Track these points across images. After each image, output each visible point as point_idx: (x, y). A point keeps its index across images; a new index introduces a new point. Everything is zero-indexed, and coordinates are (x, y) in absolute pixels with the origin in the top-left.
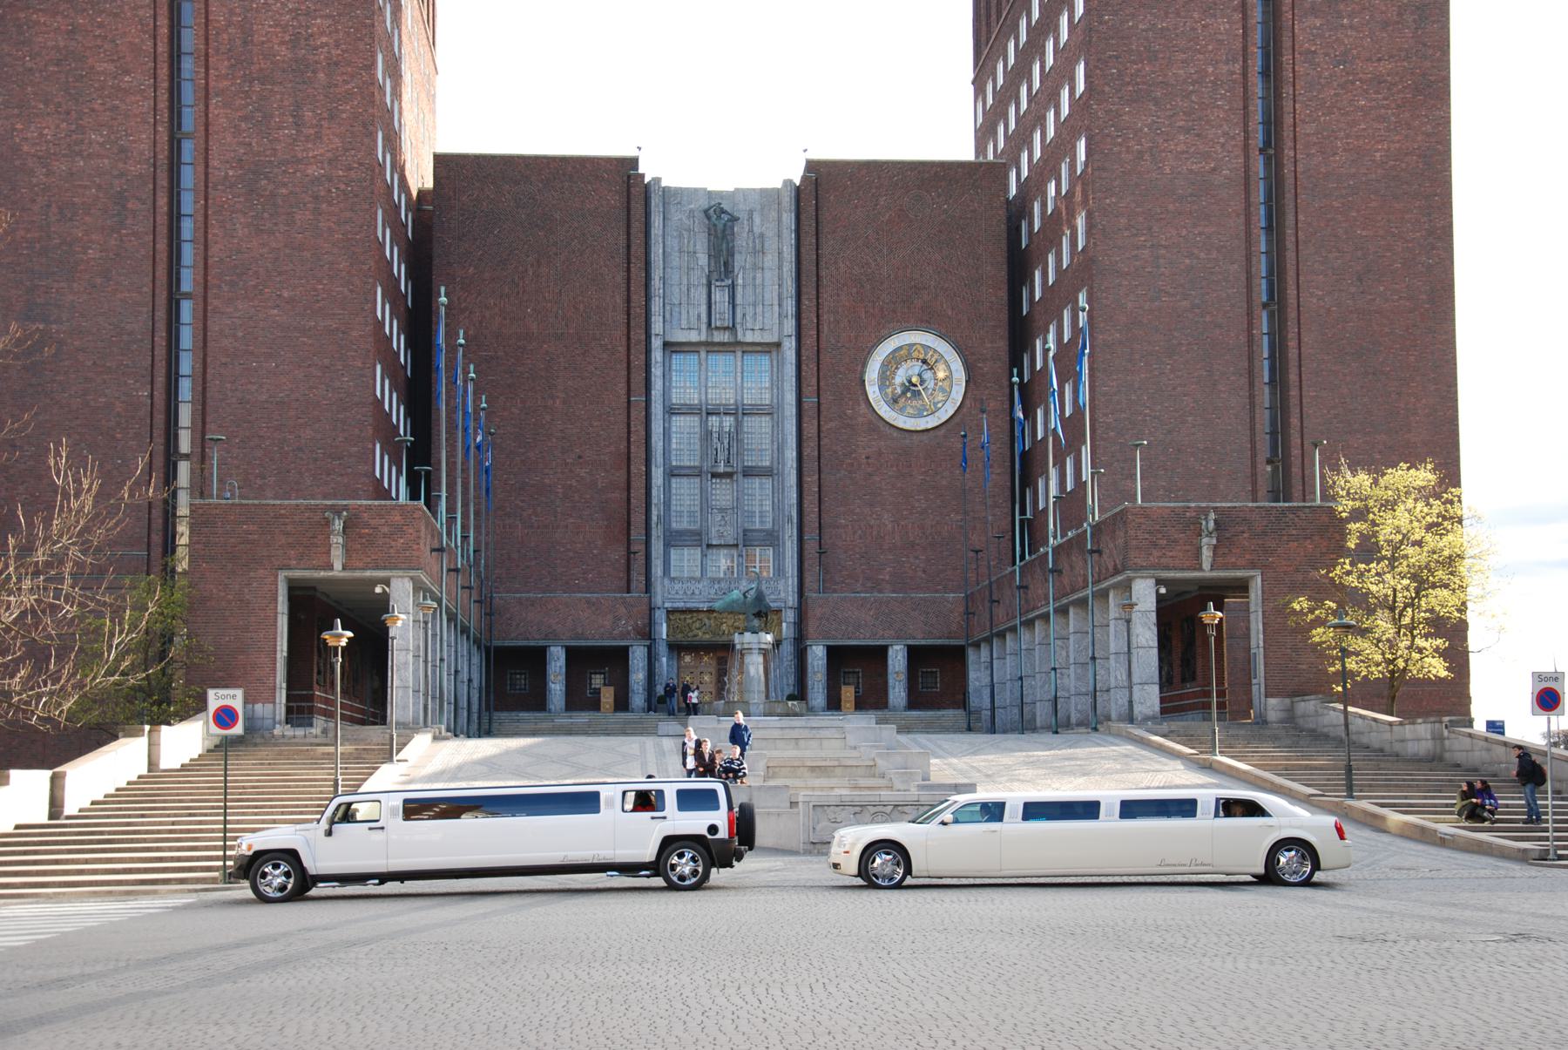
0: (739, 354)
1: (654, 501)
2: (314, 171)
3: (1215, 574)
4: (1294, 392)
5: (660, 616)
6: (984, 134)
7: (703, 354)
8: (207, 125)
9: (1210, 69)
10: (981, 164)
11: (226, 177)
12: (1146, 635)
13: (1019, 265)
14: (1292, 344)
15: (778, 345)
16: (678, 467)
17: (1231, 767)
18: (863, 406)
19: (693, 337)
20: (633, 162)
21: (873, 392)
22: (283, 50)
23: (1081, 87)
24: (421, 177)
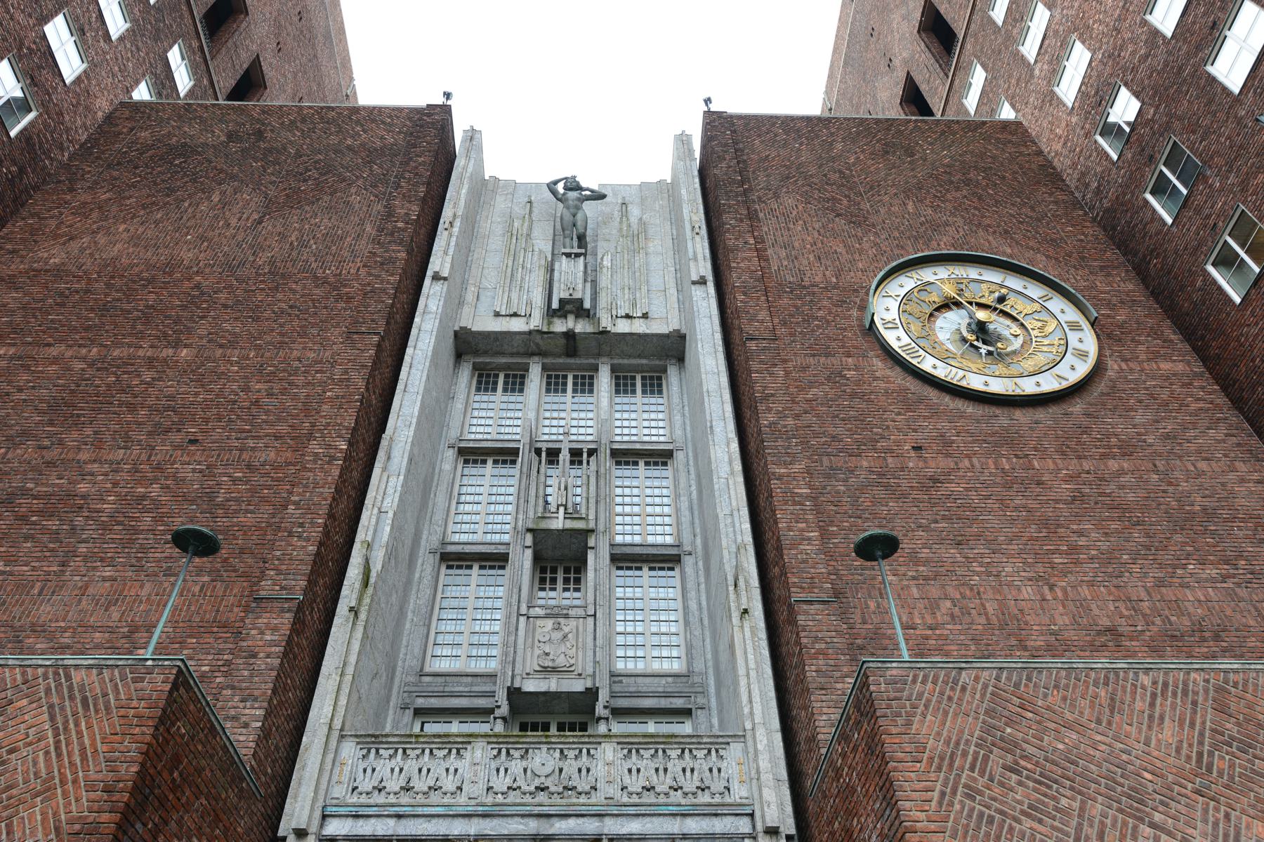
15: (673, 349)
19: (517, 325)
21: (896, 339)
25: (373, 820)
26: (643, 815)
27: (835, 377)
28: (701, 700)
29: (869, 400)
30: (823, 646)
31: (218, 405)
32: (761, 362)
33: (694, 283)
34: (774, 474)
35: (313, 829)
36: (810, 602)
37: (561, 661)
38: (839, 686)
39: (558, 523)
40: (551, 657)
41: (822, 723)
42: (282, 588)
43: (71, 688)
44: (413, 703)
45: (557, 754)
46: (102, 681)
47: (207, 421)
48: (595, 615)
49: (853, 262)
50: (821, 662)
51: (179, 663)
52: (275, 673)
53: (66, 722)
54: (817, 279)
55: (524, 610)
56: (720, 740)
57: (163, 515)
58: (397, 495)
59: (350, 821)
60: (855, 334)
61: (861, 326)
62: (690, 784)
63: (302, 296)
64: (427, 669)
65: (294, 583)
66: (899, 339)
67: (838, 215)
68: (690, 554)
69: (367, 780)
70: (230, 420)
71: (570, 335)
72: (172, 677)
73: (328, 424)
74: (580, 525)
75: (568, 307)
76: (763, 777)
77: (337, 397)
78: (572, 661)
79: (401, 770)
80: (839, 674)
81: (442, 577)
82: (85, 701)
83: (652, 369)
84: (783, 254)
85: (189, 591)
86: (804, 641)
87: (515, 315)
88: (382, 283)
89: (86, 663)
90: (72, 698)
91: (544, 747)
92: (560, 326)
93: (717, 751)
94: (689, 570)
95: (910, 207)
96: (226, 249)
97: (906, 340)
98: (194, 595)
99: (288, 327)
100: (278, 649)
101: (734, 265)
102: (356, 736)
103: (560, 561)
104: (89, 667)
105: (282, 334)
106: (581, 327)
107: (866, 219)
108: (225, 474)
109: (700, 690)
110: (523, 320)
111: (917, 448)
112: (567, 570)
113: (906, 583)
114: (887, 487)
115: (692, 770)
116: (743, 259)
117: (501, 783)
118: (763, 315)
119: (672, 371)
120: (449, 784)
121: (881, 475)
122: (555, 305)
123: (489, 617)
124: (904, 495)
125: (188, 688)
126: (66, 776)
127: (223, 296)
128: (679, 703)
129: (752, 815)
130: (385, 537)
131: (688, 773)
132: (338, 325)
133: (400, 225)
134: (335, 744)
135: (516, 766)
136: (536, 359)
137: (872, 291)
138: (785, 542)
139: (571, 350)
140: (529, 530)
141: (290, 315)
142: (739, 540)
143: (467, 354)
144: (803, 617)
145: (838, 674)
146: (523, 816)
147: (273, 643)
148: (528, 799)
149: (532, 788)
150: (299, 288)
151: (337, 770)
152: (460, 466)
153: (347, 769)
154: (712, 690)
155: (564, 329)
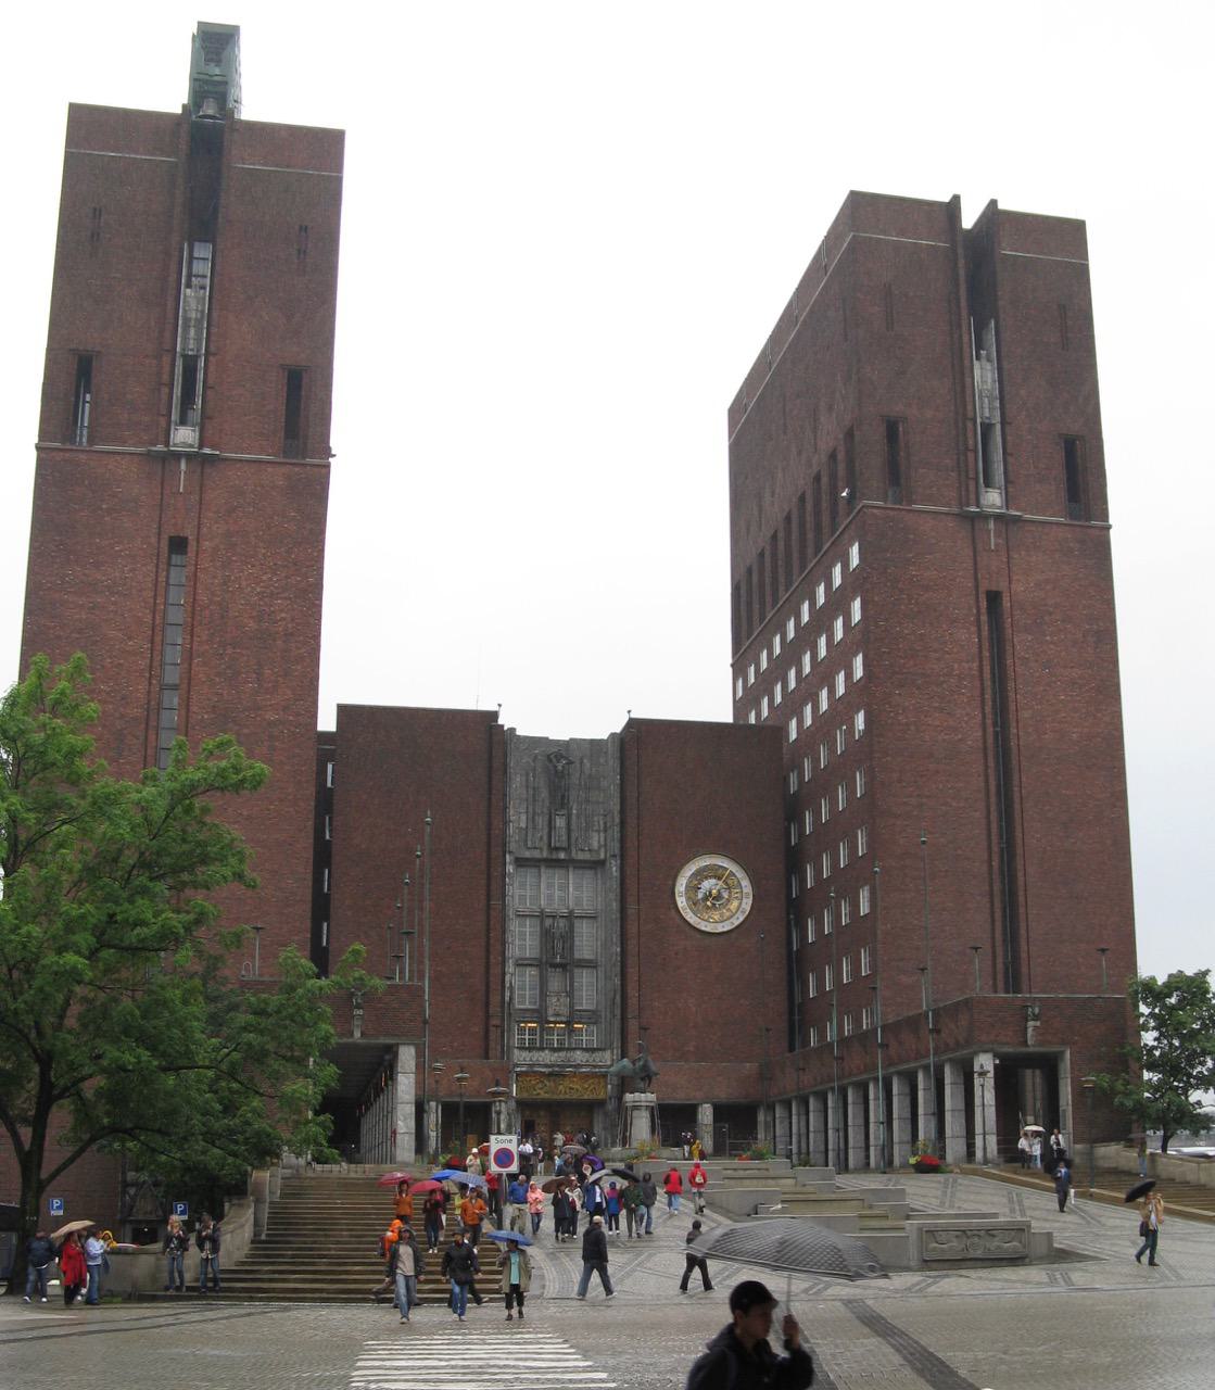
0: (571, 869)
2: (271, 716)
3: (1037, 1049)
4: (1022, 910)
6: (740, 707)
7: (542, 870)
8: (190, 679)
9: (956, 666)
10: (741, 727)
11: (202, 720)
12: (986, 1094)
13: (793, 809)
14: (1020, 874)
15: (602, 863)
16: (580, 960)
17: (1110, 1196)
18: (673, 912)
19: (537, 854)
20: (494, 715)
21: (681, 902)
22: (252, 624)
23: (859, 672)
24: (327, 722)
97: (685, 903)
120: (541, 1059)
133: (497, 832)
139: (556, 861)
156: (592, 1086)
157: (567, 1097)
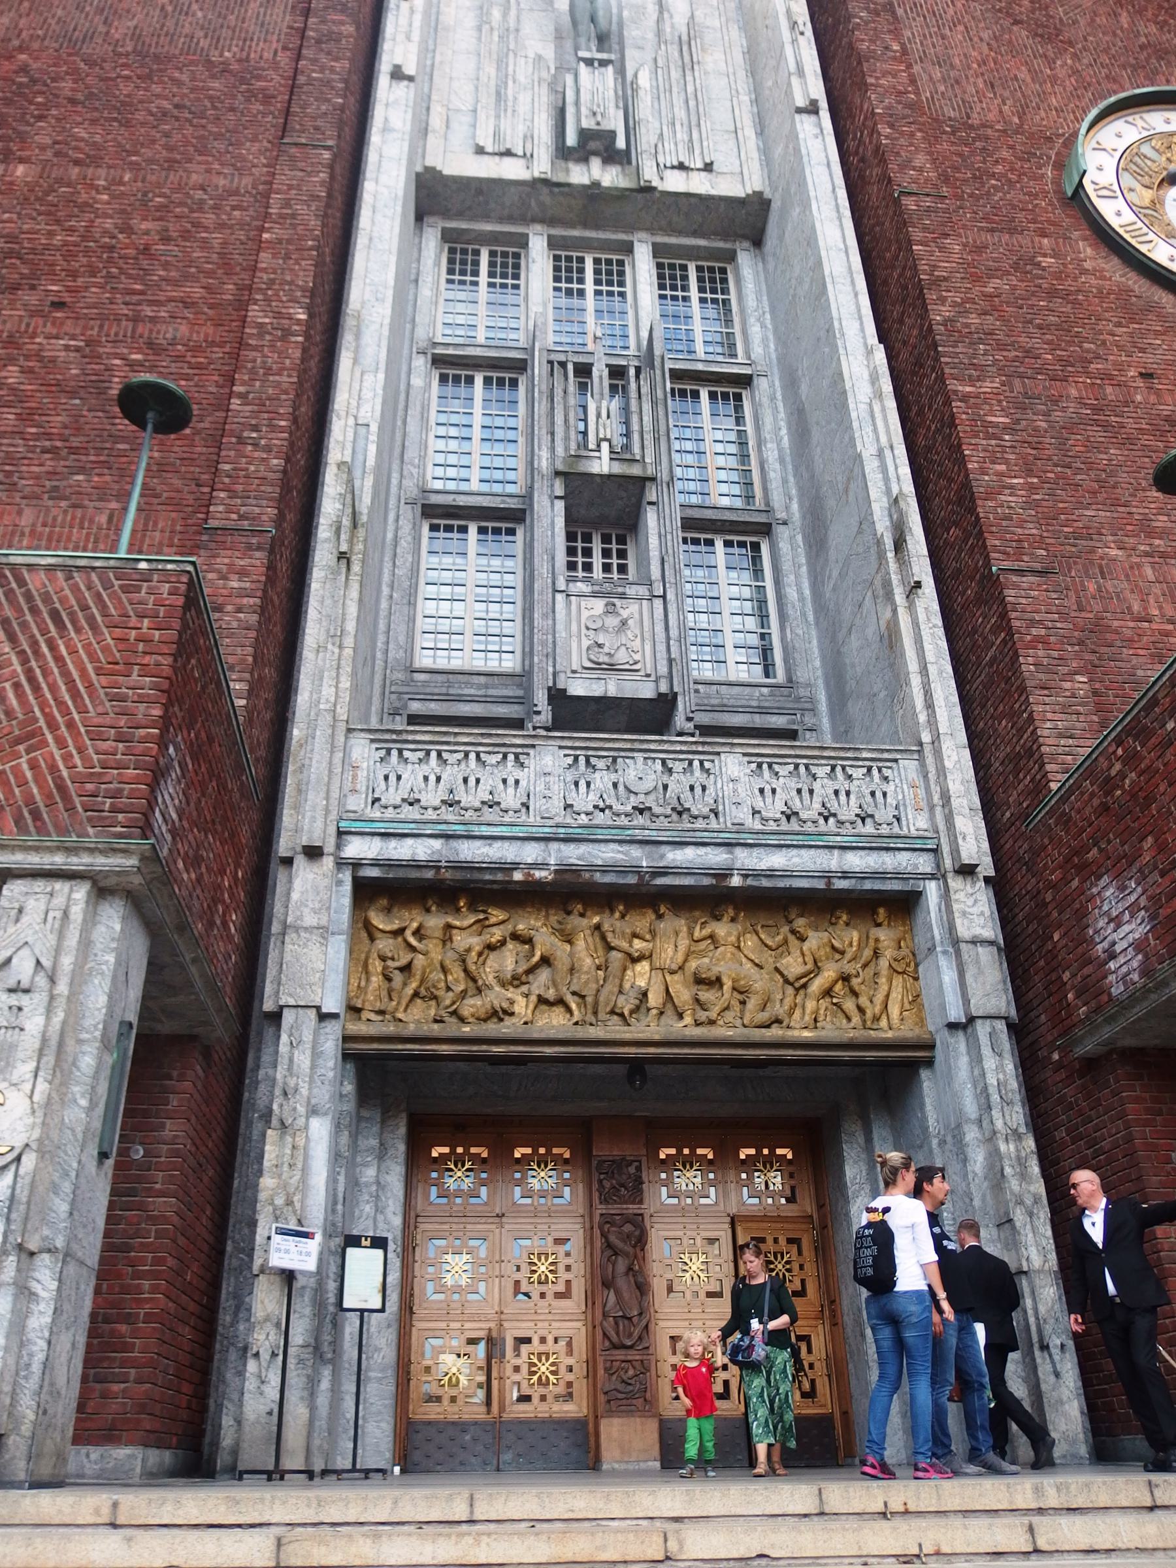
1: (335, 453)
5: (311, 899)
19: (513, 170)
21: (1116, 213)
25: (410, 841)
26: (788, 846)
27: (1024, 264)
28: (809, 720)
29: (1075, 302)
30: (1043, 632)
31: (87, 252)
32: (925, 229)
33: (799, 111)
34: (955, 392)
35: (329, 847)
36: (1020, 572)
37: (622, 657)
38: (1067, 685)
39: (602, 465)
40: (606, 650)
41: (1046, 733)
42: (242, 517)
43: (29, 596)
44: (405, 706)
45: (658, 766)
46: (75, 589)
47: (74, 275)
48: (664, 597)
49: (1043, 96)
50: (1041, 653)
51: (190, 568)
52: (253, 634)
53: (34, 644)
54: (991, 116)
55: (561, 585)
56: (886, 756)
57: (32, 412)
58: (379, 400)
59: (377, 841)
60: (1051, 204)
61: (1060, 191)
62: (848, 812)
63: (193, 90)
64: (417, 665)
65: (257, 510)
66: (1119, 214)
67: (1016, 22)
68: (785, 523)
69: (392, 790)
70: (109, 276)
71: (593, 191)
72: (183, 587)
73: (272, 281)
74: (636, 470)
75: (593, 145)
76: (955, 803)
77: (280, 241)
78: (637, 657)
79: (438, 779)
80: (1066, 670)
81: (425, 541)
82: (55, 616)
83: (713, 254)
84: (937, 74)
85: (91, 521)
86: (1016, 624)
87: (508, 153)
88: (322, 71)
89: (43, 561)
90: (34, 611)
91: (639, 756)
92: (578, 175)
93: (880, 770)
94: (784, 546)
95: (1124, 19)
96: (60, 12)
98: (100, 528)
99: (177, 137)
100: (252, 601)
101: (871, 80)
102: (369, 731)
103: (596, 524)
104: (50, 569)
105: (170, 149)
106: (610, 177)
107: (1059, 32)
108: (117, 356)
109: (807, 706)
110: (521, 163)
111: (1146, 376)
112: (606, 539)
113: (1135, 560)
114: (1106, 426)
115: (848, 793)
116: (885, 74)
117: (584, 800)
118: (920, 160)
119: (745, 260)
120: (510, 799)
121: (1096, 410)
122: (571, 140)
123: (506, 591)
124: (1130, 440)
125: (199, 613)
126: (54, 718)
127: (67, 85)
128: (779, 722)
129: (935, 851)
130: (371, 461)
131: (843, 797)
132: (255, 139)
134: (342, 739)
135: (602, 780)
136: (538, 227)
137: (1081, 137)
138: (979, 490)
140: (558, 473)
141: (177, 119)
142: (895, 490)
143: (432, 213)
144: (1012, 592)
145: (1063, 670)
146: (620, 842)
147: (243, 592)
148: (624, 821)
149: (629, 808)
150: (185, 77)
151: (349, 776)
152: (435, 382)
153: (362, 775)
154: (823, 707)
155: (586, 181)
156: (829, 974)
157: (685, 1028)
